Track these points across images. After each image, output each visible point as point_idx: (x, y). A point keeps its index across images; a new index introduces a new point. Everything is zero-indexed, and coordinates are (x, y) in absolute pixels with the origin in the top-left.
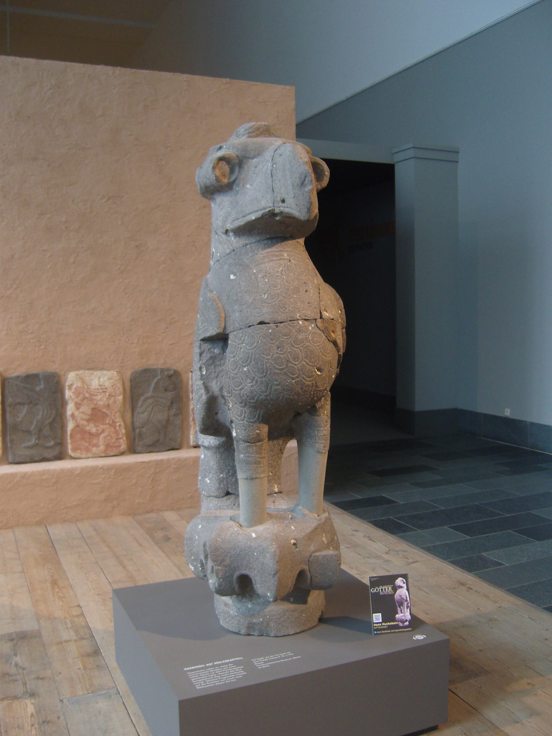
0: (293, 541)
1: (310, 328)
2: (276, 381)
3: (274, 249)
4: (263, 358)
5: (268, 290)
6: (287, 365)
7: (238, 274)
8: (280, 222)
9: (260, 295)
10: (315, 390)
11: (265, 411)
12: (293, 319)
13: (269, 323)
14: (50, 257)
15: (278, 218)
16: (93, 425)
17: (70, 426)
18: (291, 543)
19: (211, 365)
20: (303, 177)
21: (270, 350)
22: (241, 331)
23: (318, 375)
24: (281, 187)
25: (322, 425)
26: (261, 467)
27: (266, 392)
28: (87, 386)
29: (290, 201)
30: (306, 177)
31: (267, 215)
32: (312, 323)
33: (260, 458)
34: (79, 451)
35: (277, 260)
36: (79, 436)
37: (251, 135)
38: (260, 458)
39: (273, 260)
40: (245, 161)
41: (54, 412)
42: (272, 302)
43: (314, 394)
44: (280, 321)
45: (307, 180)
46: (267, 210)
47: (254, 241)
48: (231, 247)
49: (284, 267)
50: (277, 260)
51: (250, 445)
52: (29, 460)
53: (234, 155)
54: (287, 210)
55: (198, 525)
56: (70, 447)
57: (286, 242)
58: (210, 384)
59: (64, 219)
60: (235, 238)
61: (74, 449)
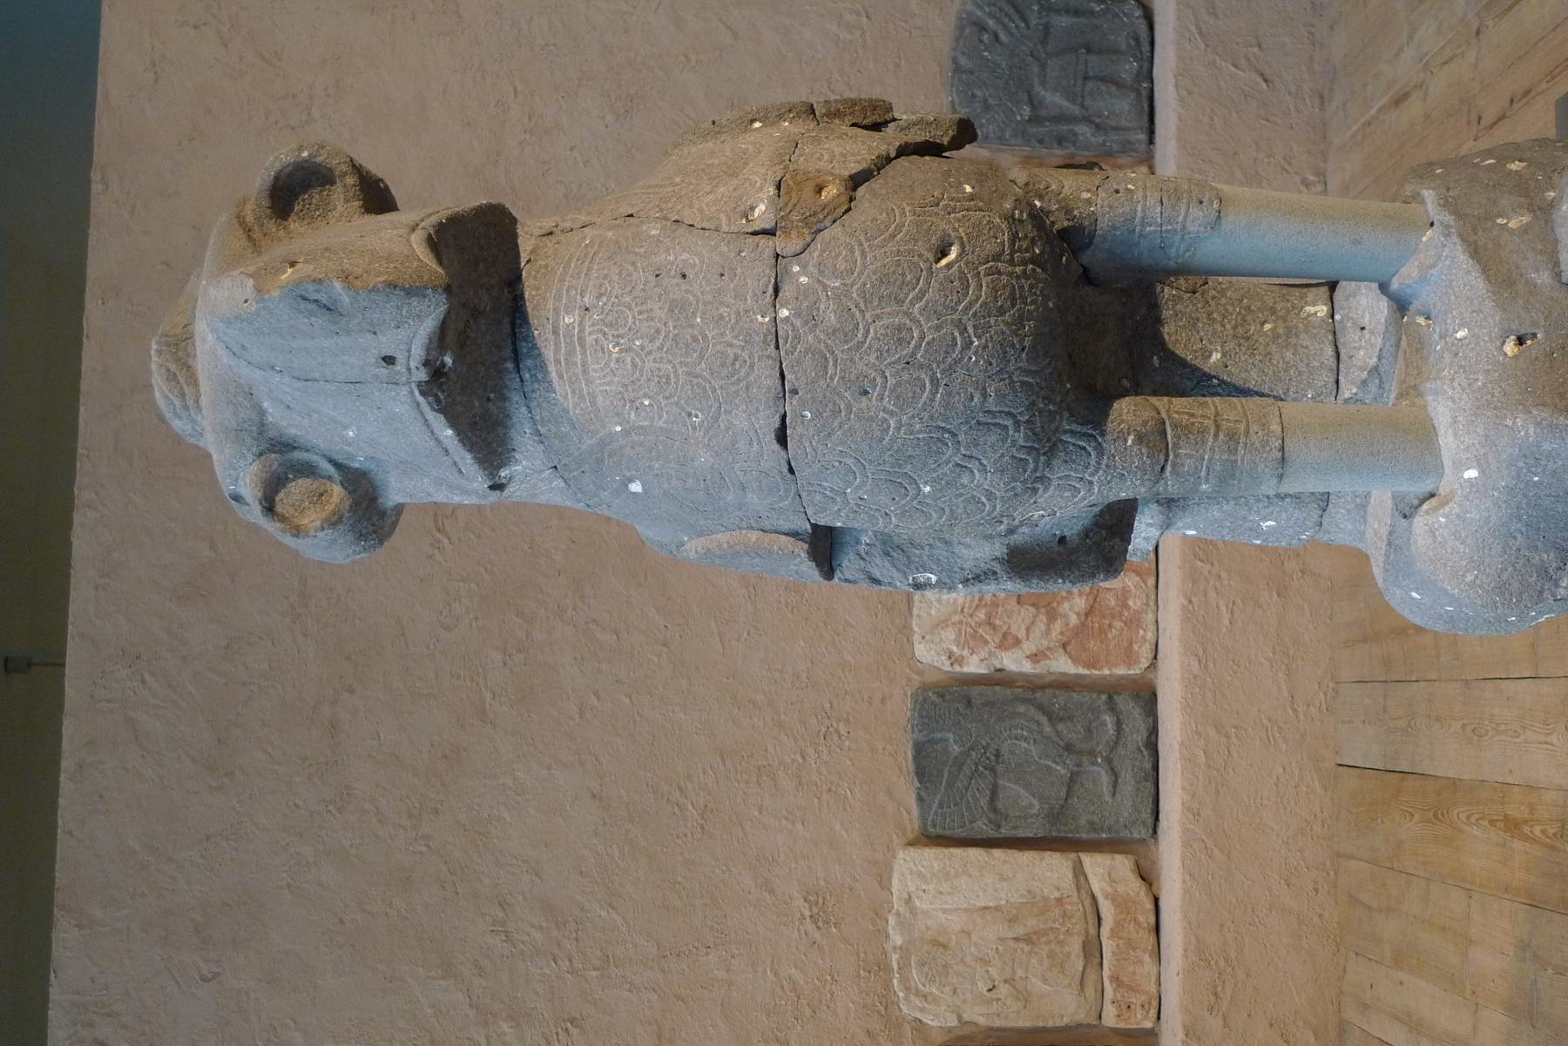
0: (1510, 348)
1: (804, 279)
2: (972, 398)
3: (549, 354)
4: (893, 440)
6: (921, 367)
9: (694, 428)
10: (1011, 262)
11: (1066, 415)
12: (771, 338)
13: (784, 416)
14: (598, 698)
15: (448, 360)
16: (1066, 605)
17: (1063, 665)
18: (1515, 357)
19: (909, 558)
20: (304, 305)
21: (872, 419)
22: (804, 495)
23: (960, 256)
24: (343, 363)
25: (1127, 209)
26: (1247, 432)
27: (1006, 427)
28: (955, 612)
29: (388, 342)
30: (305, 299)
31: (438, 400)
32: (787, 271)
33: (1216, 436)
34: (1136, 647)
35: (584, 353)
36: (1092, 644)
37: (190, 403)
38: (1216, 436)
40: (271, 434)
41: (1022, 709)
42: (716, 399)
43: (1024, 263)
44: (778, 382)
46: (420, 399)
47: (524, 409)
49: (605, 334)
50: (584, 353)
51: (1174, 465)
52: (1150, 785)
53: (255, 467)
54: (418, 352)
56: (1121, 671)
57: (529, 307)
58: (968, 565)
59: (498, 657)
61: (1129, 657)
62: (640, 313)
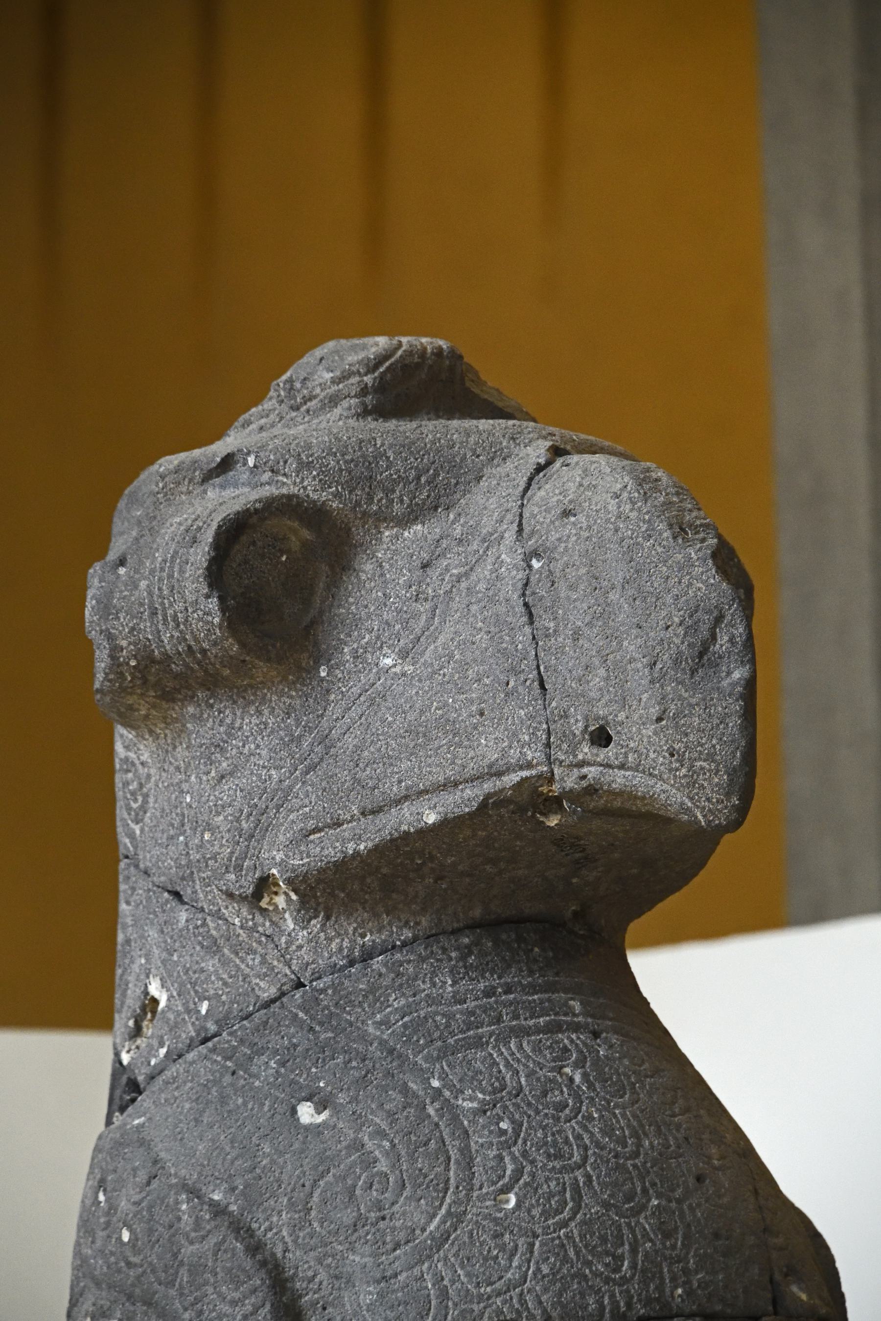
5: (518, 1173)
7: (342, 1098)
8: (560, 840)
20: (707, 619)
30: (719, 619)
39: (526, 1032)
45: (723, 639)
46: (514, 778)
47: (408, 934)
48: (279, 966)
54: (619, 779)
60: (304, 923)
62: (635, 1116)
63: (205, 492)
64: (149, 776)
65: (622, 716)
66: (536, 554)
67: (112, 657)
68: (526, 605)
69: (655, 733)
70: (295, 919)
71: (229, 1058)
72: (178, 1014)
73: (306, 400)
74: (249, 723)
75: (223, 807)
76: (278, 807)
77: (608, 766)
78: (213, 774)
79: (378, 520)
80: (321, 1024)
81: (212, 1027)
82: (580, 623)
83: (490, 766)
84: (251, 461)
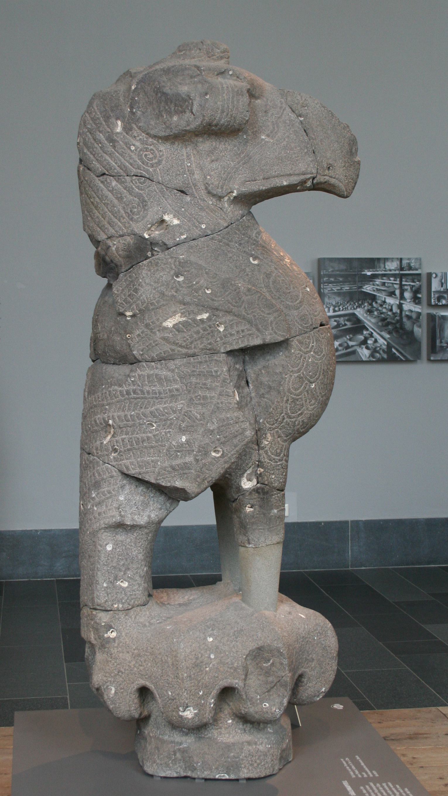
55: (205, 639)
63: (217, 78)
64: (163, 155)
65: (335, 165)
66: (300, 116)
67: (202, 122)
68: (305, 130)
69: (343, 170)
70: (228, 205)
71: (221, 242)
72: (189, 227)
73: (213, 55)
74: (222, 146)
75: (214, 170)
76: (235, 173)
77: (331, 177)
78: (209, 159)
79: (253, 97)
80: (244, 235)
81: (210, 233)
82: (321, 138)
83: (303, 171)
84: (231, 73)
